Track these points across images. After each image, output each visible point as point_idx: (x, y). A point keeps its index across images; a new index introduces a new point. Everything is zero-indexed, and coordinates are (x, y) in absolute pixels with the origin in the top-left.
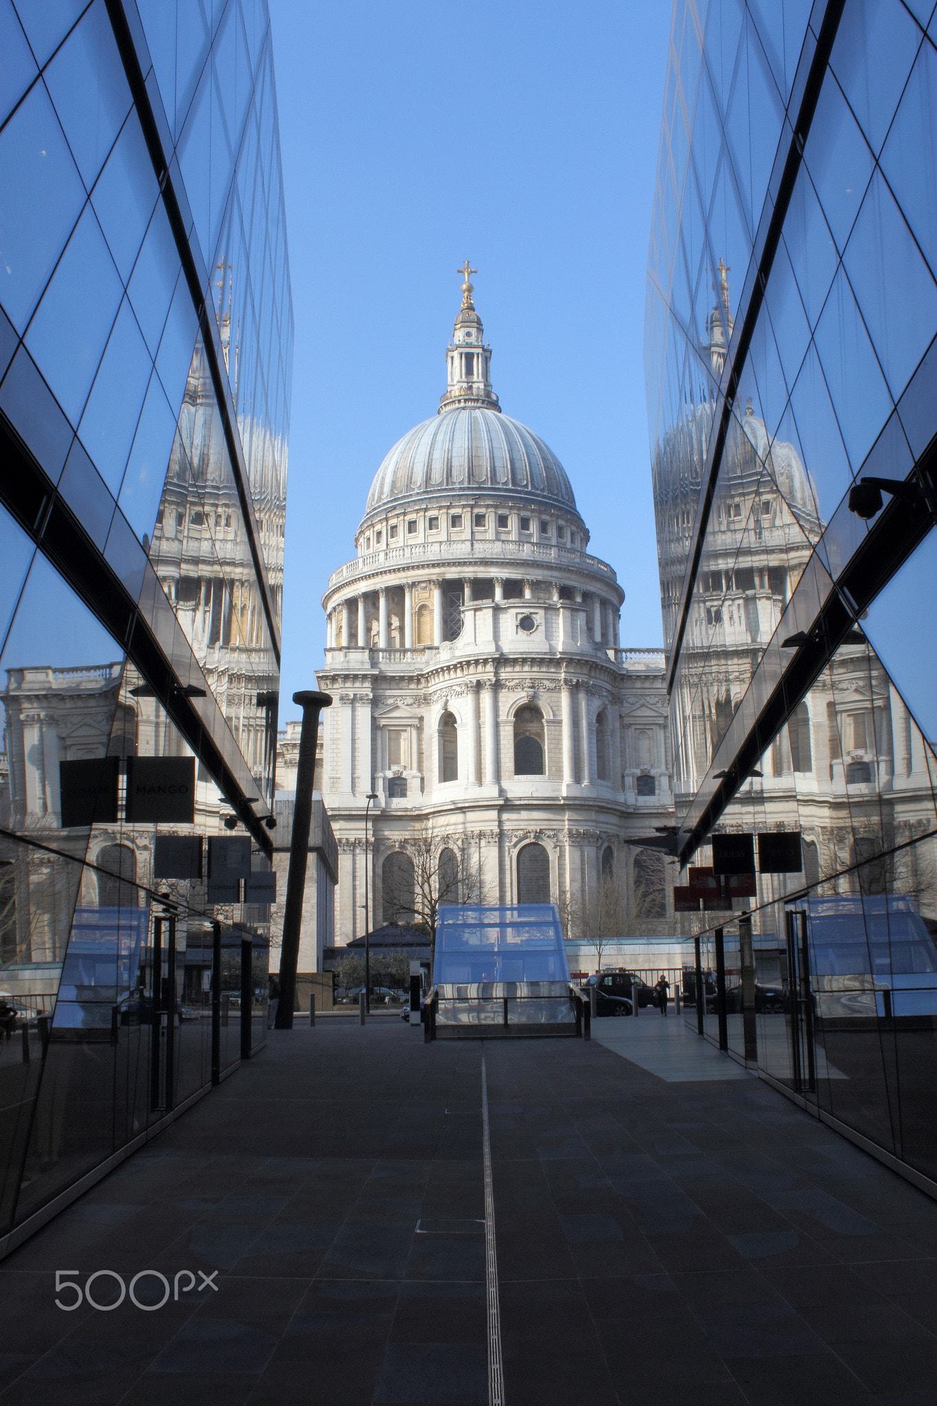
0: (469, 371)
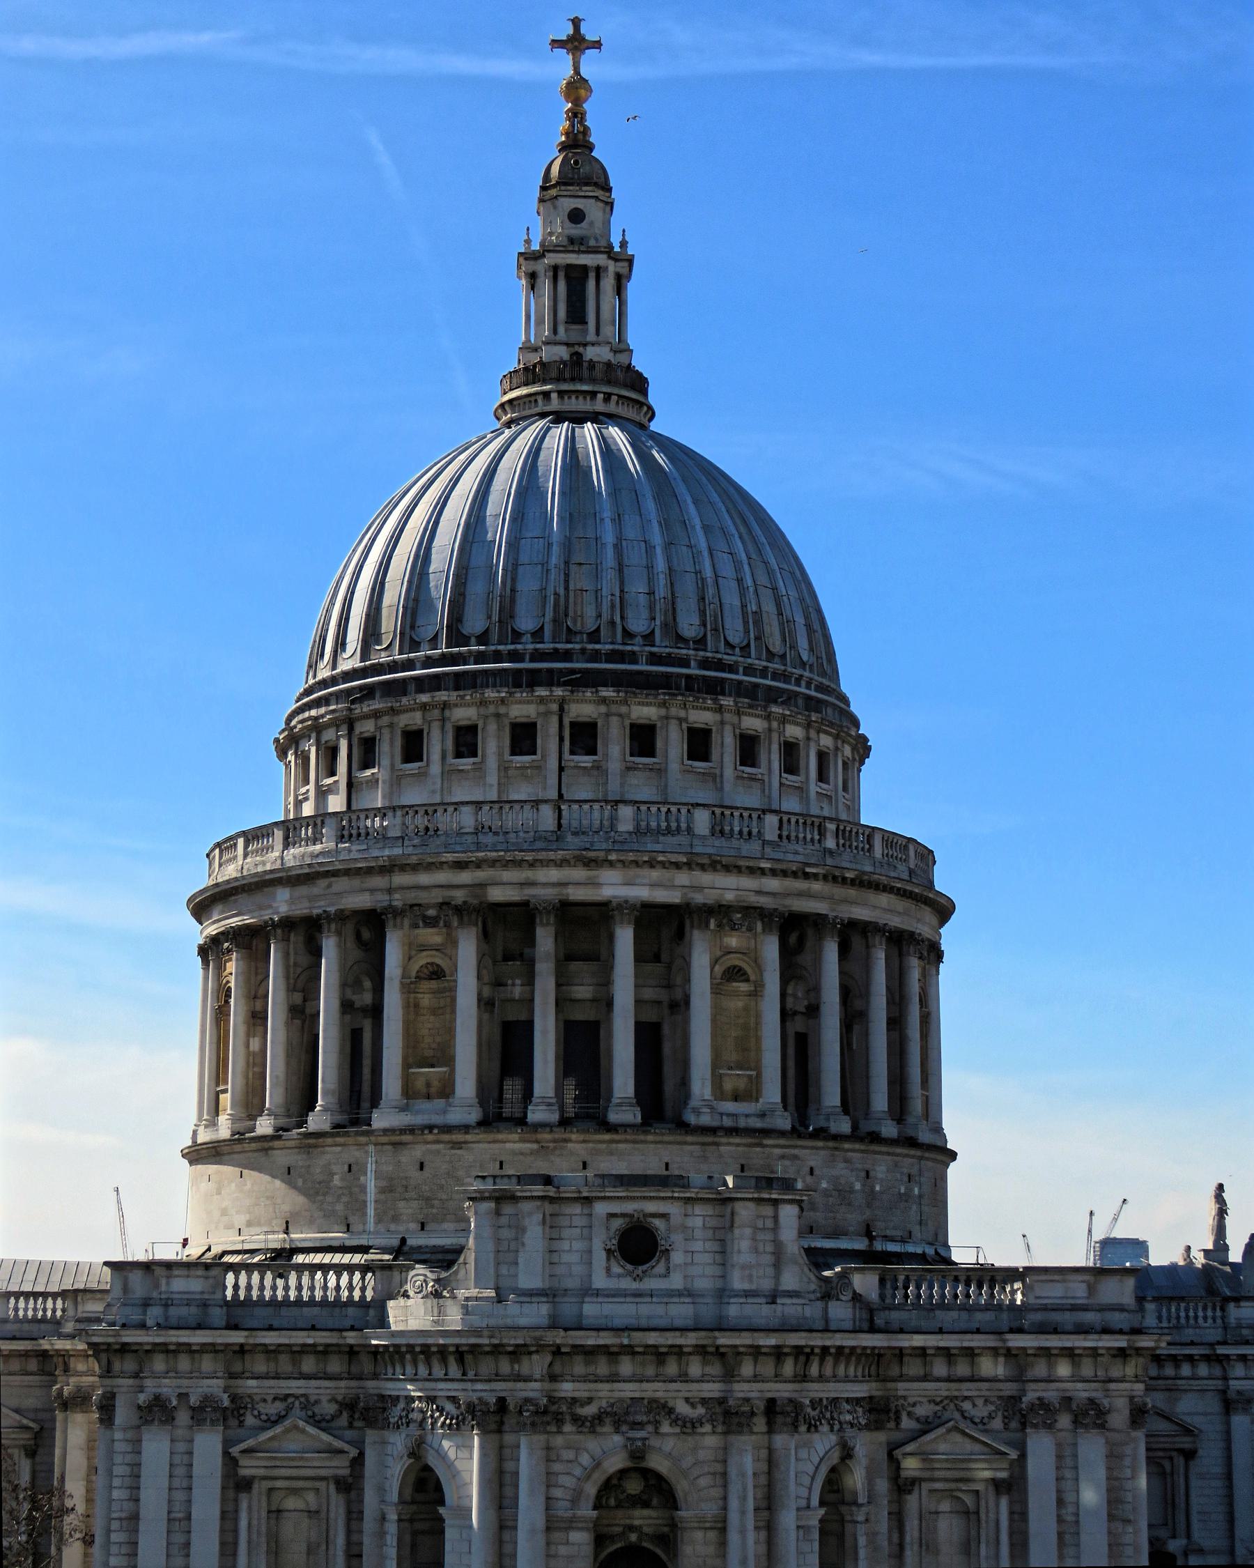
0: (576, 314)
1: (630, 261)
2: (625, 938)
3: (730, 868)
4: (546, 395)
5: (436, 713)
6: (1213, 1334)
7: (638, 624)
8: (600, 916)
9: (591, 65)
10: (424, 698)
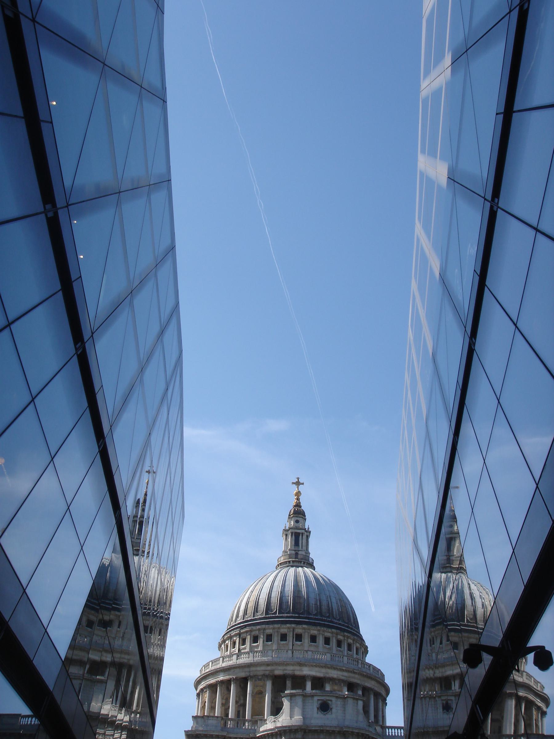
1: (310, 532)
4: (289, 562)
5: (262, 631)
10: (258, 627)
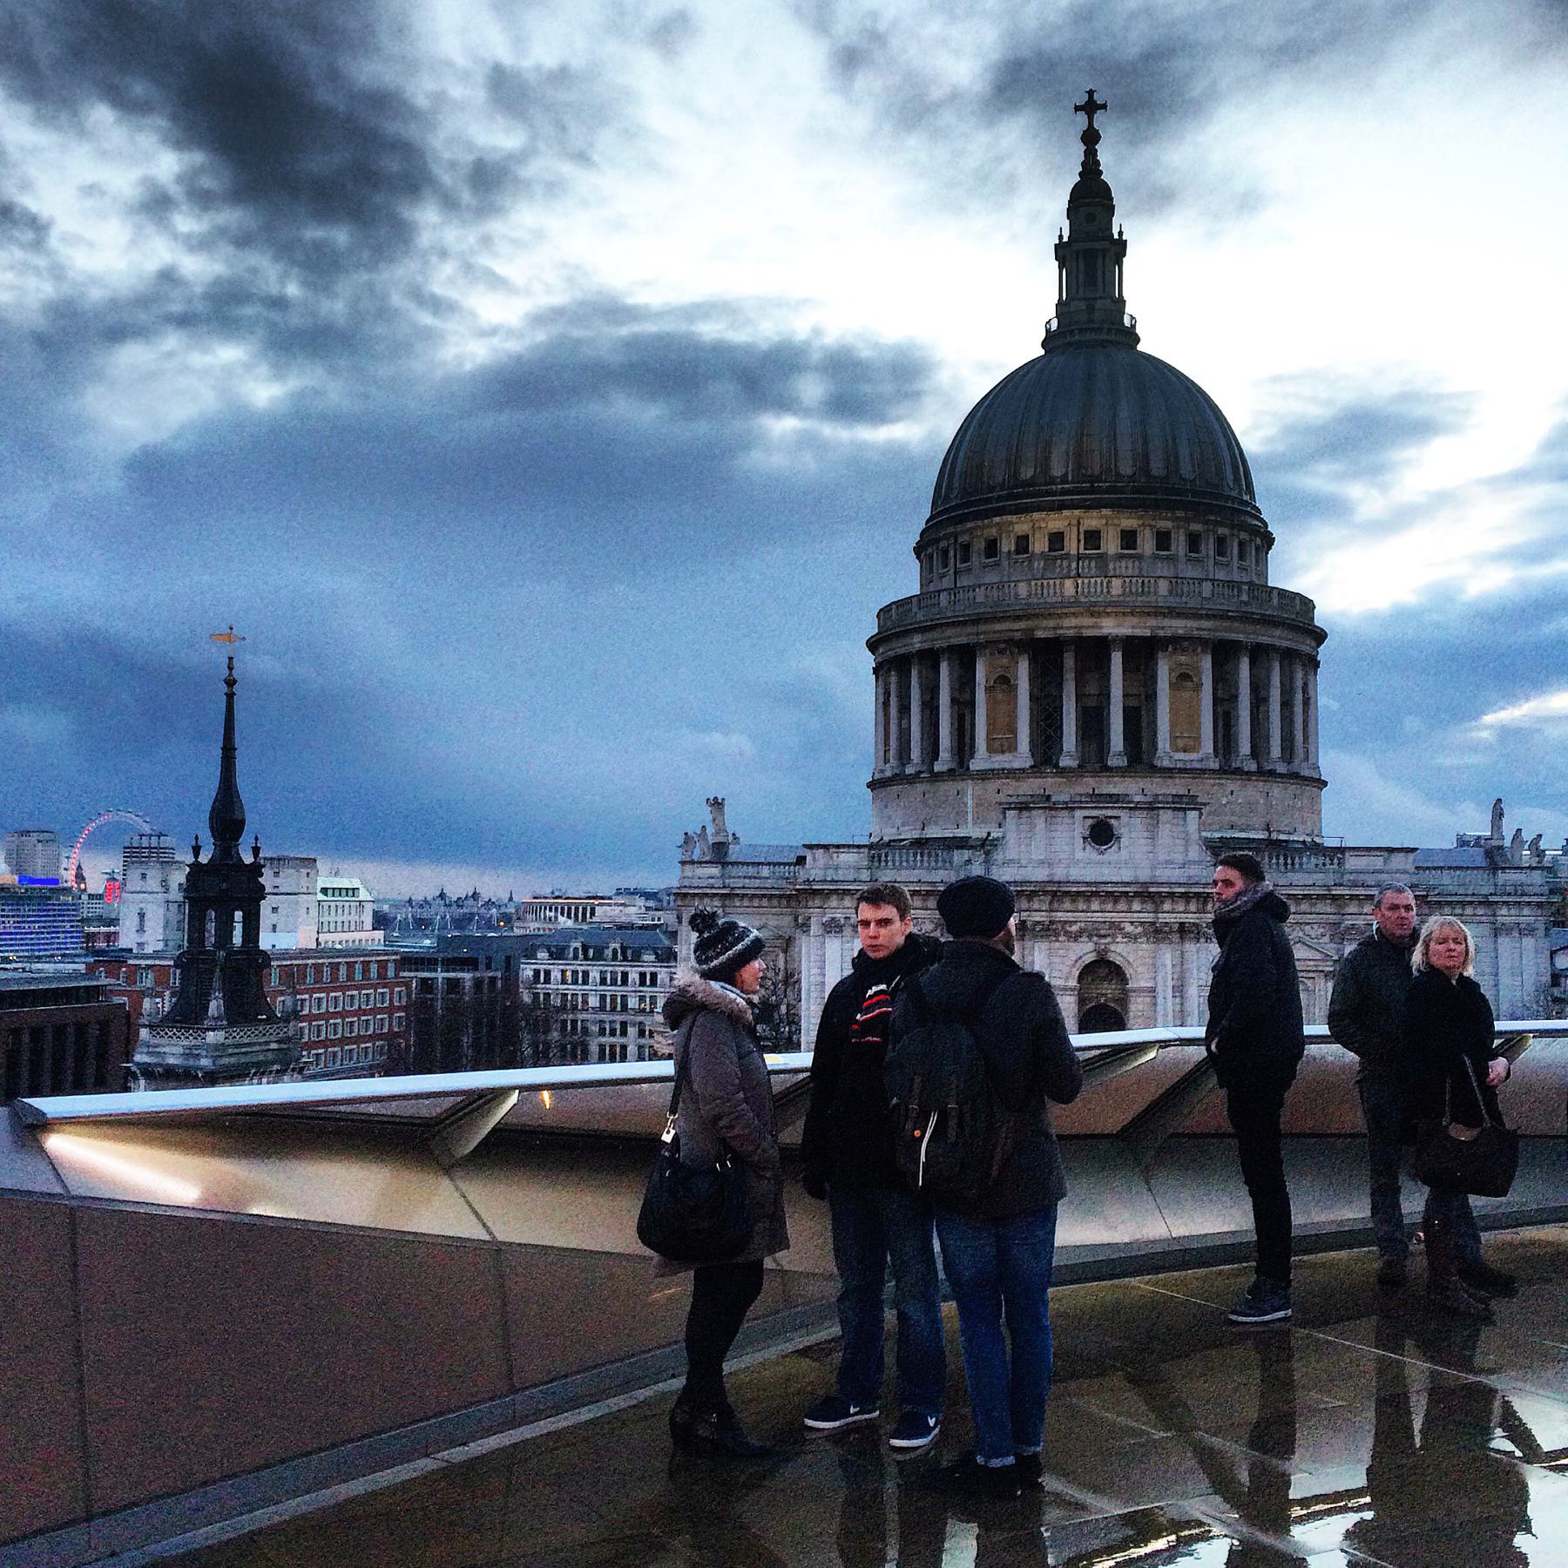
2: (1117, 659)
3: (1179, 615)
6: (1485, 891)
7: (1126, 469)
8: (1101, 646)
9: (1100, 119)
